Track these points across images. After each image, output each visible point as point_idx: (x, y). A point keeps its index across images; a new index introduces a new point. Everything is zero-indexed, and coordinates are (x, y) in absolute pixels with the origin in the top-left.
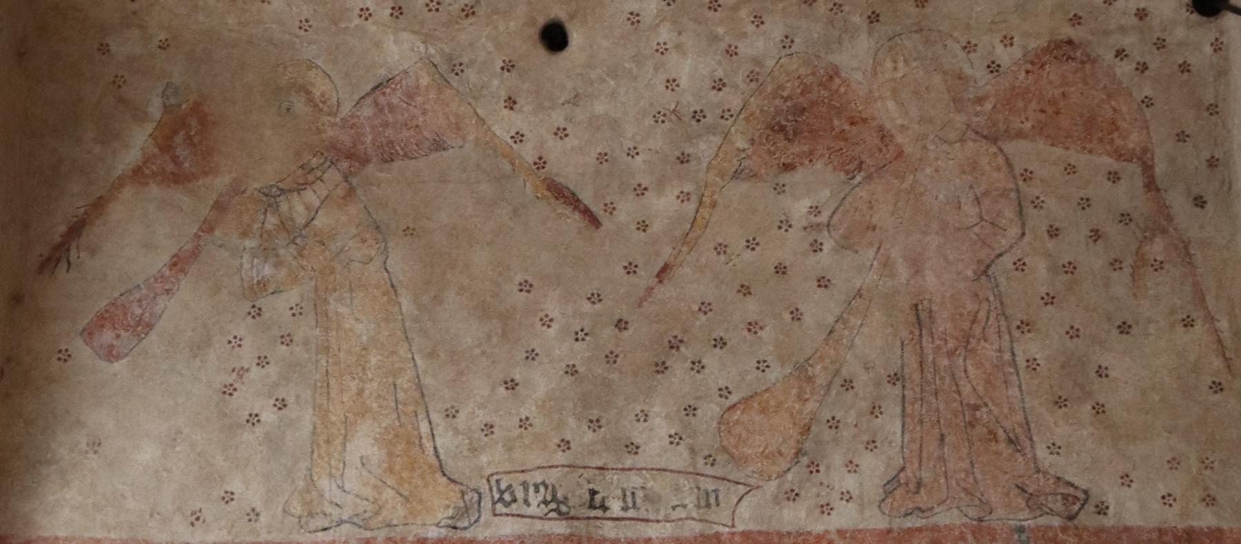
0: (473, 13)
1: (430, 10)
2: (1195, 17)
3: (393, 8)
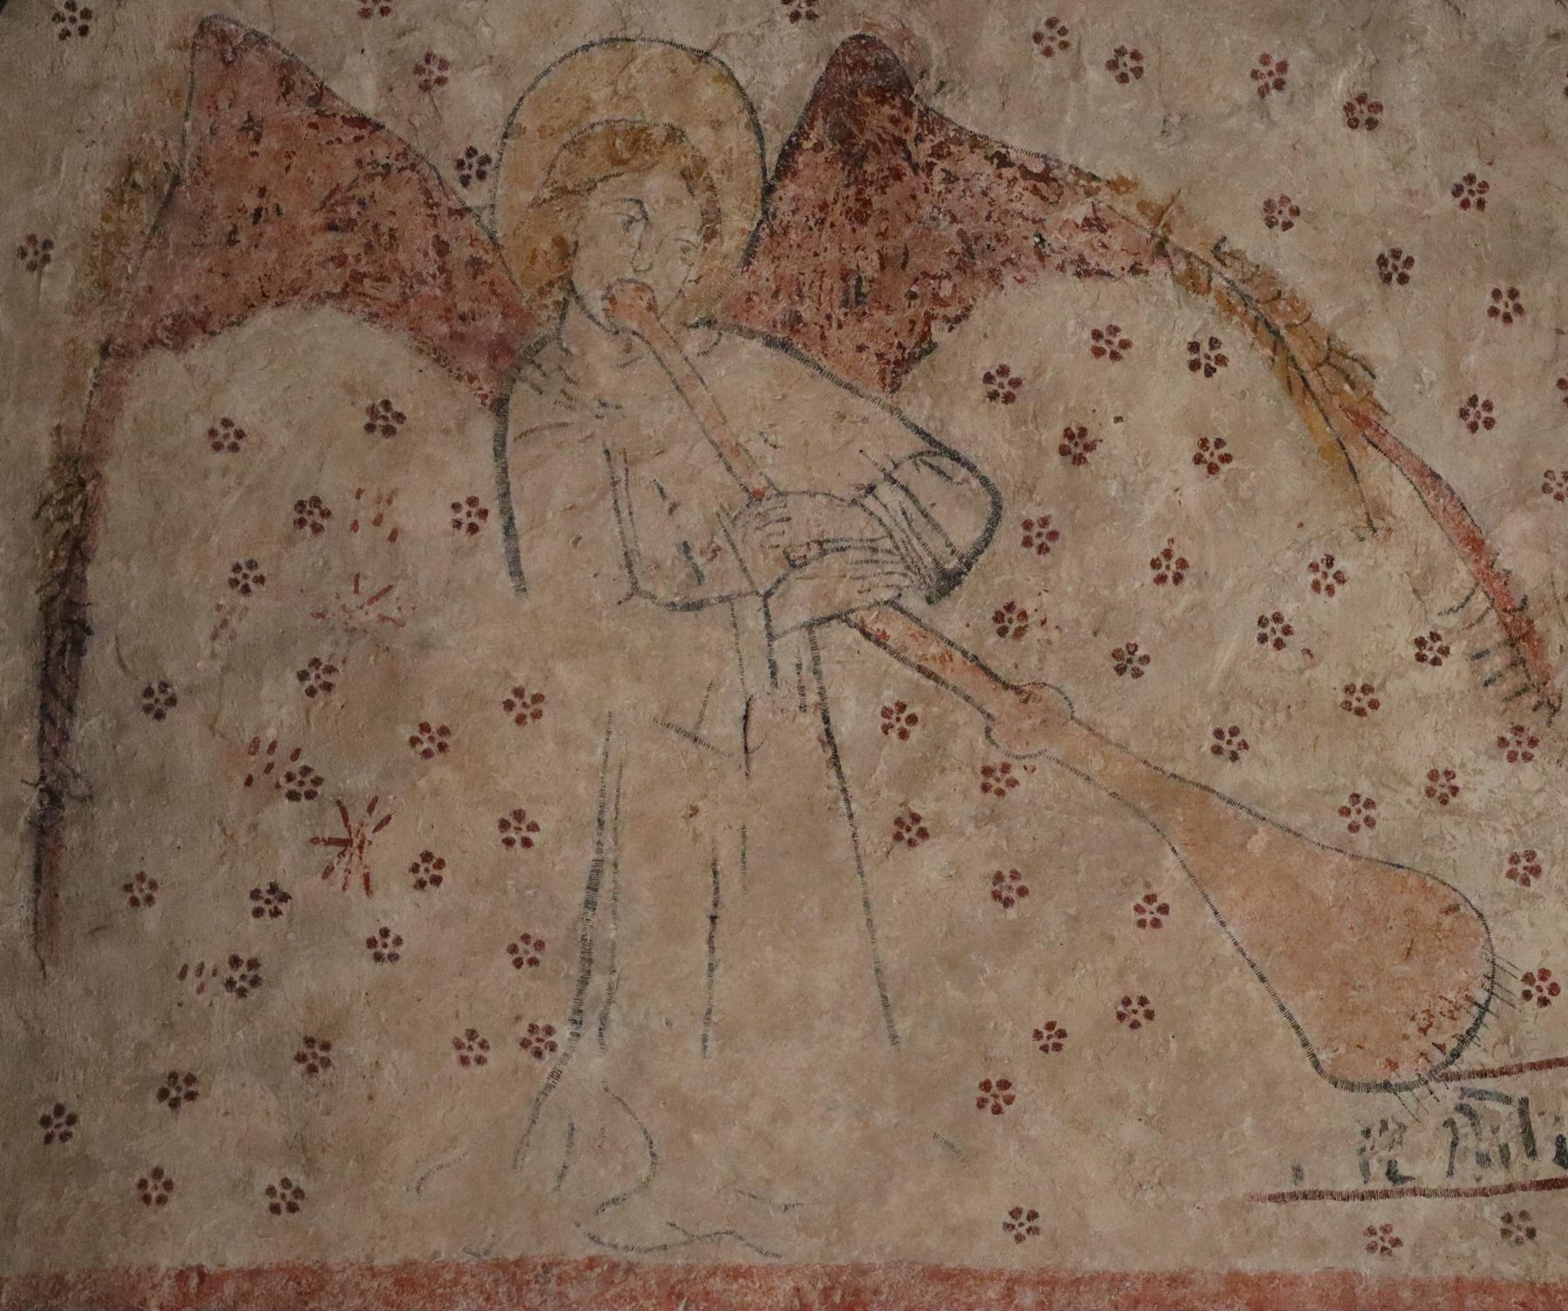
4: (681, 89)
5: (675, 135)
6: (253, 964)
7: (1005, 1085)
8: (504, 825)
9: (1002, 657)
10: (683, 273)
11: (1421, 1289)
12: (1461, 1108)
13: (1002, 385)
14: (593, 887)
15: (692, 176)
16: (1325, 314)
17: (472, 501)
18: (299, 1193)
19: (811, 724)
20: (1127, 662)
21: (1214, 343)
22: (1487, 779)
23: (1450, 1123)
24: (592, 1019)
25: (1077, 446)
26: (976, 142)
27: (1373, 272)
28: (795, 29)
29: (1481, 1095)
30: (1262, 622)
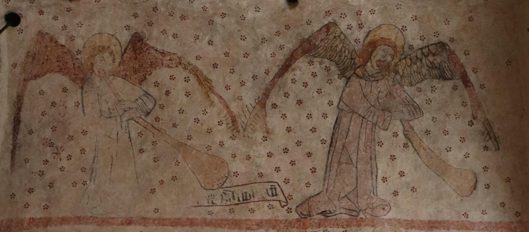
0: (326, 12)
1: (345, 14)
2: (18, 12)
3: (360, 15)
4: (110, 41)
5: (109, 47)
6: (43, 172)
7: (154, 189)
8: (81, 151)
9: (156, 125)
10: (110, 68)
11: (216, 220)
12: (223, 193)
13: (156, 84)
14: (94, 160)
15: (111, 53)
16: (205, 73)
17: (78, 102)
18: (48, 206)
19: (127, 135)
20: (174, 125)
21: (188, 77)
22: (228, 143)
23: (222, 195)
24: (93, 180)
25: (168, 93)
26: (153, 48)
27: (212, 66)
28: (126, 31)
29: (226, 191)
30: (195, 119)
